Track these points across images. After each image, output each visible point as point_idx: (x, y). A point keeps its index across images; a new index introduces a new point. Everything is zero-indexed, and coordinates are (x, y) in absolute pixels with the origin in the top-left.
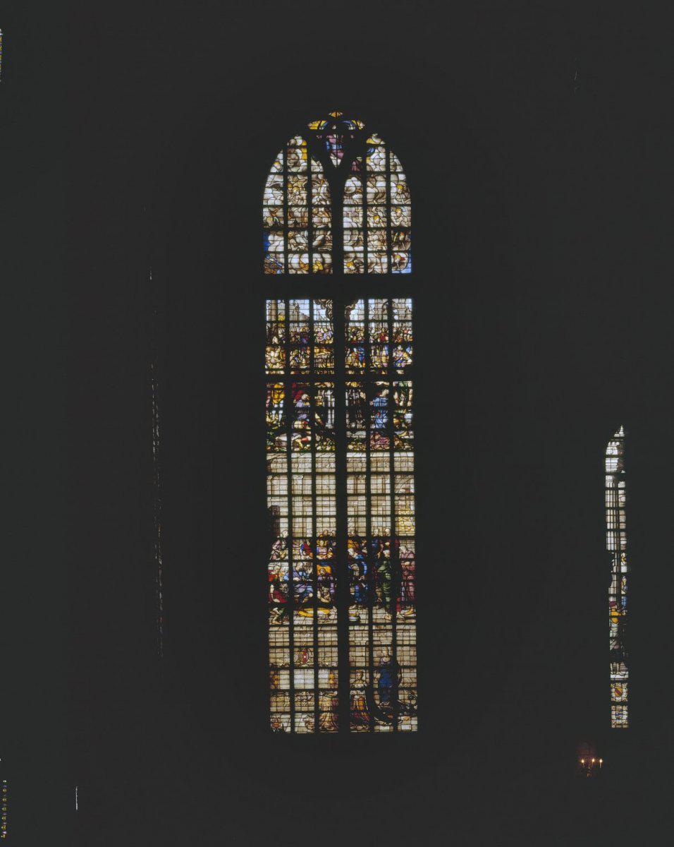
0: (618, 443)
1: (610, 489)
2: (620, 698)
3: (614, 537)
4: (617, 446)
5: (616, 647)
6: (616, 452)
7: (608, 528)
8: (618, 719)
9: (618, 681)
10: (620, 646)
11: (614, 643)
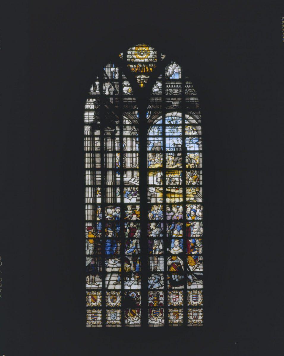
0: (94, 100)
1: (88, 136)
2: (95, 304)
3: (91, 175)
4: (94, 102)
5: (92, 263)
6: (93, 107)
7: (86, 167)
8: (94, 320)
9: (94, 290)
10: (95, 262)
11: (91, 260)
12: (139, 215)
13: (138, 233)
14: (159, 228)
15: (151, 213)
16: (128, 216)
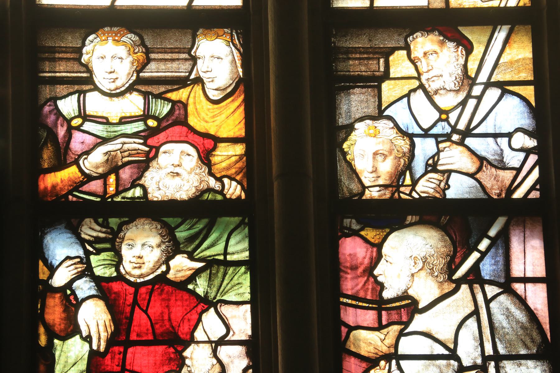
12: (234, 141)
13: (224, 352)
14: (491, 290)
15: (384, 125)
16: (87, 153)
